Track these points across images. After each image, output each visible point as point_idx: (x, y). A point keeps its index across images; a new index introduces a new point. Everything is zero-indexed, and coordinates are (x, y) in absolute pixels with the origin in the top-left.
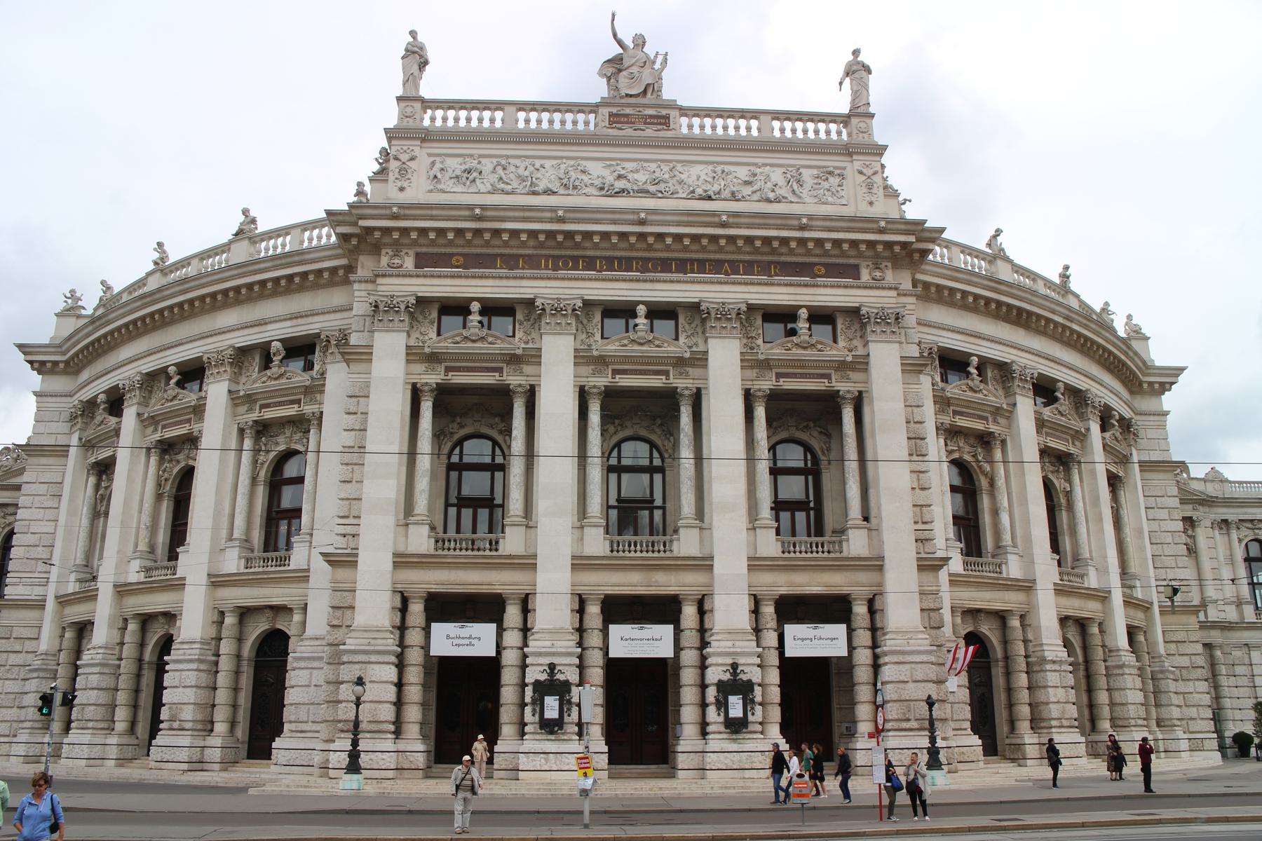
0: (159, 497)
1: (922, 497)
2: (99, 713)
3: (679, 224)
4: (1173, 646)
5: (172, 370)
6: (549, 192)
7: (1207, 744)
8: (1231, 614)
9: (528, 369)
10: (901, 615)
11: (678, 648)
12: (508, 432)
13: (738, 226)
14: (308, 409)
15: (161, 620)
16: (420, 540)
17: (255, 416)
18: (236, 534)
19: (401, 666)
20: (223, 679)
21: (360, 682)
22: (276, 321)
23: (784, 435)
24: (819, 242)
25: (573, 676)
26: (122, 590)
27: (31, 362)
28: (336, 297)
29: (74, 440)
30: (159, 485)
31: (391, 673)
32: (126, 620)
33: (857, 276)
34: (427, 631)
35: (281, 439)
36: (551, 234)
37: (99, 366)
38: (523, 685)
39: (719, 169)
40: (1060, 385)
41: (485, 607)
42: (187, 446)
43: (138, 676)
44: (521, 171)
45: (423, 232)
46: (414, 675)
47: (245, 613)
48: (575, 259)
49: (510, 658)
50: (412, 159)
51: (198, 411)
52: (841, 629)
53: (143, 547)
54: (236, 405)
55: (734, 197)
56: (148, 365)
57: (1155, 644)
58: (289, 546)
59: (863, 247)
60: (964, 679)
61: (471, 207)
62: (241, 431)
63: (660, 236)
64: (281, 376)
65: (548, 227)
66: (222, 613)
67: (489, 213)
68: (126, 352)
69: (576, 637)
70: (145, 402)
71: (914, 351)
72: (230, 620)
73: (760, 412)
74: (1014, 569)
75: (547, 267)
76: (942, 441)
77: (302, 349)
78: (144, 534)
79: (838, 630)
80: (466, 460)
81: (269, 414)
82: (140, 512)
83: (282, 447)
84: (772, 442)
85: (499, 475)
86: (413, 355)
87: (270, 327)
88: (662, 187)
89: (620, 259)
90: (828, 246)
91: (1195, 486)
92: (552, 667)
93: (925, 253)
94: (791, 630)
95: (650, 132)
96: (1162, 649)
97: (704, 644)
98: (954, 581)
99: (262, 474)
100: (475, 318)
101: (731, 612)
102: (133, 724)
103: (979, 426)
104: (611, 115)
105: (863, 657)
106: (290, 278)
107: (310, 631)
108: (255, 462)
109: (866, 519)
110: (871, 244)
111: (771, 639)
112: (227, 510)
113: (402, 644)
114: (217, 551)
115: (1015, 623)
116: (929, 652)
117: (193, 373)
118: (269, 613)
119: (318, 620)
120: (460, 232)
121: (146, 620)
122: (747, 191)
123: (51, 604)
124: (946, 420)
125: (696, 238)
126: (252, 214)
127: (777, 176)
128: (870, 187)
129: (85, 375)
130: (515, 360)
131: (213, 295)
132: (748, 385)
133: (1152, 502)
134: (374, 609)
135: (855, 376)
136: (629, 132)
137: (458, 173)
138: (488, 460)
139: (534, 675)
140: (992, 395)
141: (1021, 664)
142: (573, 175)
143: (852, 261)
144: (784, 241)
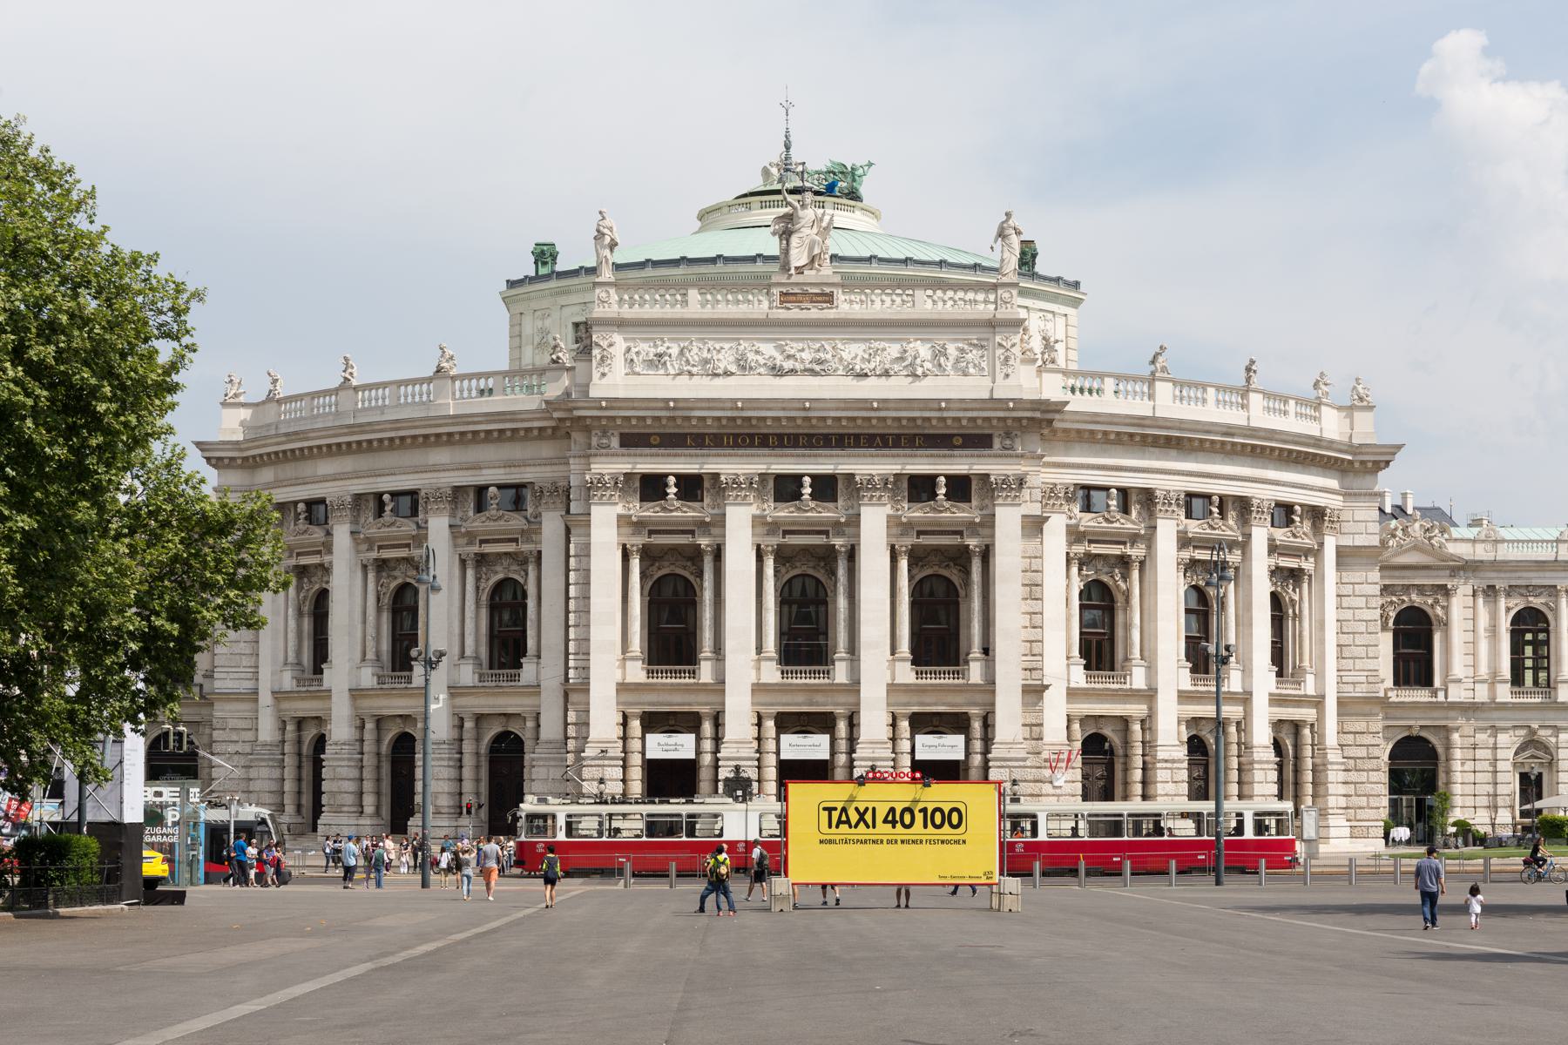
0: (379, 610)
1: (1033, 634)
2: (349, 799)
3: (837, 409)
4: (1351, 736)
5: (386, 497)
6: (727, 374)
7: (1373, 832)
8: (1482, 694)
9: (714, 531)
10: (1009, 726)
11: (833, 753)
12: (700, 575)
13: (887, 409)
14: (525, 547)
15: (399, 720)
16: (637, 672)
17: (476, 549)
18: (468, 652)
19: (624, 767)
20: (467, 773)
21: (602, 781)
22: (492, 467)
23: (929, 572)
24: (958, 419)
25: (752, 773)
27: (208, 459)
28: (546, 450)
30: (378, 600)
31: (618, 773)
33: (990, 446)
34: (643, 739)
35: (499, 568)
36: (733, 419)
37: (289, 470)
38: (716, 781)
39: (876, 345)
40: (1216, 499)
41: (686, 722)
42: (402, 567)
43: (378, 767)
44: (705, 355)
45: (628, 418)
46: (636, 773)
47: (479, 718)
48: (752, 436)
49: (707, 759)
50: (611, 345)
51: (420, 538)
52: (961, 738)
53: (370, 655)
55: (886, 374)
56: (360, 486)
57: (1322, 736)
58: (520, 666)
59: (995, 422)
60: (1078, 774)
61: (667, 400)
62: (463, 562)
63: (824, 419)
64: (500, 518)
65: (729, 414)
67: (681, 405)
68: (326, 467)
69: (755, 744)
70: (355, 521)
71: (1035, 509)
72: (469, 725)
73: (903, 564)
74: (1138, 679)
75: (728, 446)
76: (1075, 570)
77: (517, 495)
78: (370, 644)
79: (960, 739)
82: (364, 622)
83: (500, 576)
84: (918, 578)
86: (623, 520)
87: (484, 472)
88: (825, 367)
89: (789, 435)
90: (964, 422)
91: (1452, 549)
92: (737, 768)
93: (1050, 422)
94: (920, 739)
95: (814, 313)
96: (1331, 738)
97: (852, 751)
98: (1073, 694)
100: (672, 490)
101: (874, 724)
102: (378, 808)
103: (1115, 550)
104: (782, 294)
105: (977, 760)
106: (501, 431)
107: (544, 735)
108: (477, 588)
109: (986, 651)
110: (1004, 419)
111: (905, 745)
112: (457, 630)
113: (625, 751)
115: (1137, 727)
116: (1024, 760)
117: (411, 502)
118: (503, 719)
119: (550, 728)
120: (658, 419)
121: (380, 721)
122: (896, 367)
123: (265, 698)
124: (1080, 549)
125: (854, 419)
126: (449, 352)
127: (924, 351)
128: (1007, 359)
129: (266, 475)
130: (704, 526)
131: (426, 437)
132: (894, 541)
133: (1348, 590)
134: (604, 723)
135: (985, 531)
136: (795, 313)
137: (651, 356)
139: (724, 773)
140: (1132, 523)
141: (1138, 762)
142: (751, 356)
143: (987, 432)
144: (929, 419)
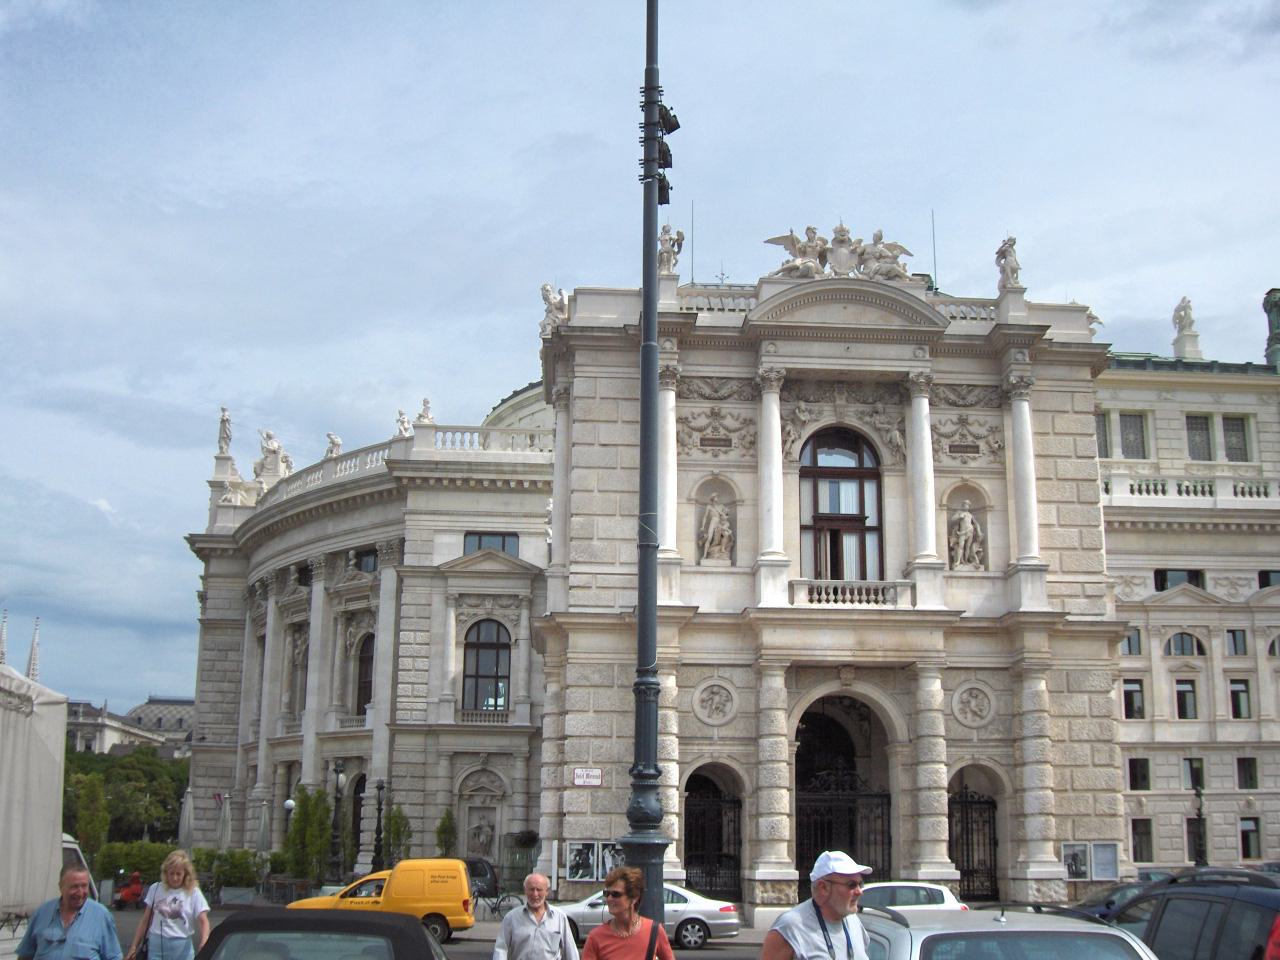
14: (373, 603)
17: (342, 608)
26: (274, 744)
29: (248, 615)
32: (276, 766)
54: (331, 599)
62: (336, 619)
66: (327, 762)
77: (366, 555)
80: (483, 639)
81: (353, 606)
83: (363, 632)
85: (503, 654)
99: (353, 652)
114: (323, 715)
117: (305, 574)
118: (356, 762)
138: (495, 640)
